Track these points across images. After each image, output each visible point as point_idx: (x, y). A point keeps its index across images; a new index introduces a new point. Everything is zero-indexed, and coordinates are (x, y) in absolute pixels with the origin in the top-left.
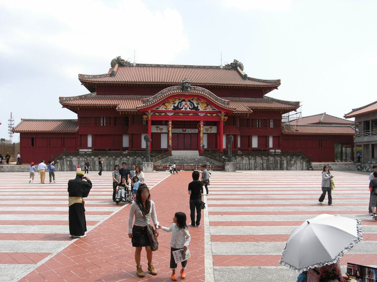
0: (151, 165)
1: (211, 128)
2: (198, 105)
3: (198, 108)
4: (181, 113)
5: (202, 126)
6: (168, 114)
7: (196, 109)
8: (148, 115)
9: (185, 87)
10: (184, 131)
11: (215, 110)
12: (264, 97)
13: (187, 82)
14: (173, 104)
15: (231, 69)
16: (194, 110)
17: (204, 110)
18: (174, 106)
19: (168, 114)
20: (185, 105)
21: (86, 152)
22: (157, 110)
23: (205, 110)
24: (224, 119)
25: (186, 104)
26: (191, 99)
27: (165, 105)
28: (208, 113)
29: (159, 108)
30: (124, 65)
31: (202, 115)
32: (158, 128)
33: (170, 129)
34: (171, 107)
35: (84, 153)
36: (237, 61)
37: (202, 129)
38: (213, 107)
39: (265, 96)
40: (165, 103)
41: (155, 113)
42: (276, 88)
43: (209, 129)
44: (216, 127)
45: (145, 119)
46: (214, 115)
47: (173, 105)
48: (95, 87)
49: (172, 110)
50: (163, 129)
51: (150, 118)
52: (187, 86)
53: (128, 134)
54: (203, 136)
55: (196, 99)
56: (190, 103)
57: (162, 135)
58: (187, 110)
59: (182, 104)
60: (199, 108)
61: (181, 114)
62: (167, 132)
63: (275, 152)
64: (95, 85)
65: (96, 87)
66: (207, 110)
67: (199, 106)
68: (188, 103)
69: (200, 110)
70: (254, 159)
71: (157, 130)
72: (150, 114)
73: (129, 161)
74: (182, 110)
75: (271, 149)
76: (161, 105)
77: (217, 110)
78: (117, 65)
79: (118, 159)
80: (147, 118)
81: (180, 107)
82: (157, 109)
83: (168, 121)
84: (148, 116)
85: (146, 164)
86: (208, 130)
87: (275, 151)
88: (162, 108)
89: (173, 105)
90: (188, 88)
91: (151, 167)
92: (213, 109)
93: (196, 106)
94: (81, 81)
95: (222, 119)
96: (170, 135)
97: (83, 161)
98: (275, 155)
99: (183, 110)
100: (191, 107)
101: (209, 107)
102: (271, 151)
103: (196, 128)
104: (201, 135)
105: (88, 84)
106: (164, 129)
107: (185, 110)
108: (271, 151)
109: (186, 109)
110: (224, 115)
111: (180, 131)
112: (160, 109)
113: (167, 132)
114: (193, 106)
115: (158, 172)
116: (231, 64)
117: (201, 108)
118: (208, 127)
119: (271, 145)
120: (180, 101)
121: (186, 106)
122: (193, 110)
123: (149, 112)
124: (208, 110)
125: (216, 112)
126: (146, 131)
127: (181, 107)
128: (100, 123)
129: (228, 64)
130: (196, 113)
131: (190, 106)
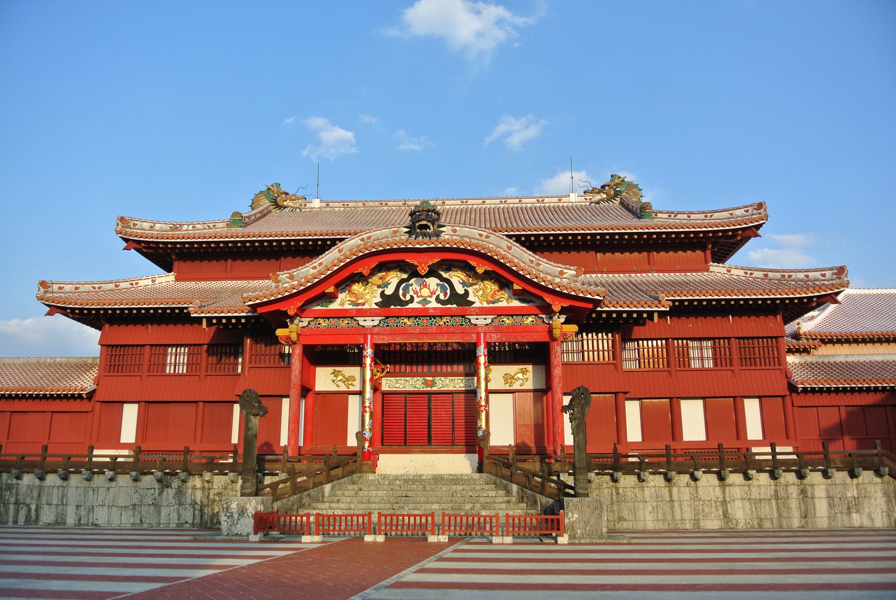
4: (409, 317)
5: (482, 360)
7: (462, 300)
10: (426, 383)
14: (379, 287)
15: (603, 200)
16: (455, 306)
17: (488, 303)
19: (361, 323)
23: (493, 303)
30: (285, 207)
31: (481, 321)
35: (108, 460)
36: (619, 177)
42: (750, 232)
44: (544, 367)
47: (381, 290)
56: (439, 282)
58: (427, 306)
59: (412, 285)
60: (471, 298)
61: (406, 320)
63: (774, 453)
67: (470, 290)
70: (688, 485)
71: (333, 381)
73: (212, 492)
74: (410, 306)
75: (757, 443)
79: (176, 483)
81: (404, 295)
83: (361, 349)
86: (512, 377)
87: (773, 449)
88: (342, 302)
89: (381, 290)
90: (427, 227)
93: (460, 290)
94: (126, 240)
97: (56, 489)
98: (774, 469)
99: (414, 305)
100: (442, 297)
102: (755, 450)
107: (420, 306)
108: (755, 450)
109: (425, 301)
112: (335, 306)
114: (448, 291)
116: (603, 187)
119: (754, 429)
120: (405, 276)
121: (425, 292)
122: (449, 306)
124: (504, 304)
127: (408, 298)
129: (594, 189)
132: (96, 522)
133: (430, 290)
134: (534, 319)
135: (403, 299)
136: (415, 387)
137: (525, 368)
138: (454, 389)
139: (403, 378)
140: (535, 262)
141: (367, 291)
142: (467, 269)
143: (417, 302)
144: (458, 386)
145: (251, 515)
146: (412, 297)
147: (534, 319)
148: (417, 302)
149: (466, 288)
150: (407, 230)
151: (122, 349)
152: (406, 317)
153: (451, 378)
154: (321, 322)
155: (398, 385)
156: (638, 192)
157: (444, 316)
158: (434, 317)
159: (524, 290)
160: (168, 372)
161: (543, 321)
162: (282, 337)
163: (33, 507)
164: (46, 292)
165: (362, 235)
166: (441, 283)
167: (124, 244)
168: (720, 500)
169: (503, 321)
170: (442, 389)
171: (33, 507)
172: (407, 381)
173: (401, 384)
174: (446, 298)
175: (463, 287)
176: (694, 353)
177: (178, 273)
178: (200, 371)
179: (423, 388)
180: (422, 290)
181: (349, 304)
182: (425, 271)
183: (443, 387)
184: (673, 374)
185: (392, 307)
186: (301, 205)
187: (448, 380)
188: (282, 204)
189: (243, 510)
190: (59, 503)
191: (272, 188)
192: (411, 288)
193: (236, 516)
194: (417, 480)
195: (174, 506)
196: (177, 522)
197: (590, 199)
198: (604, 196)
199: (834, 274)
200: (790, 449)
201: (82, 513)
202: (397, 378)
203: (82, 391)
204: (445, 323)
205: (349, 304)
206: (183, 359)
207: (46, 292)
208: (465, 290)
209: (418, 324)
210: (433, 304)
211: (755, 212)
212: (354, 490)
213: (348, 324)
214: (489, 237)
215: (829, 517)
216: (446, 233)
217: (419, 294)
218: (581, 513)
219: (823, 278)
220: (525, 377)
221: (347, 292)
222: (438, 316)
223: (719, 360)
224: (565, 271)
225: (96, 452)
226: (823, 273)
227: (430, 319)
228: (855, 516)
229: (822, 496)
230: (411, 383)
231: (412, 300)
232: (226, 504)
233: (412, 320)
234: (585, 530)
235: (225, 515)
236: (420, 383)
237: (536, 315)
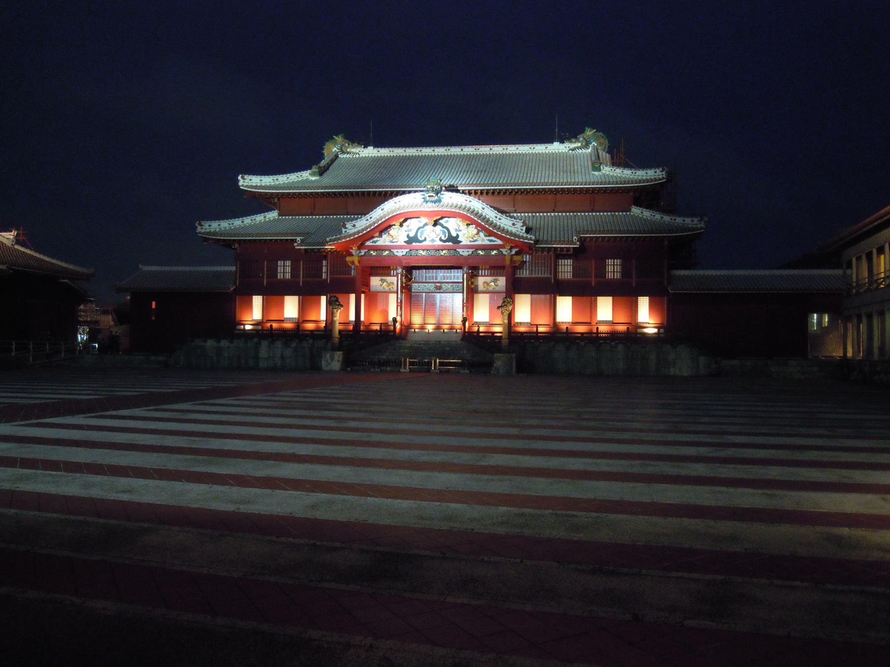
0: (339, 357)
3: (458, 239)
6: (395, 251)
11: (495, 243)
14: (406, 231)
15: (578, 148)
16: (451, 243)
18: (408, 236)
19: (395, 254)
23: (474, 241)
29: (377, 241)
32: (383, 283)
41: (369, 250)
43: (491, 282)
47: (407, 233)
61: (421, 252)
67: (460, 233)
69: (461, 244)
74: (424, 243)
77: (499, 242)
80: (353, 263)
81: (421, 237)
91: (338, 361)
100: (443, 238)
107: (430, 243)
109: (433, 241)
114: (447, 235)
122: (447, 243)
127: (423, 239)
130: (455, 249)
143: (430, 241)
144: (455, 289)
148: (430, 241)
149: (457, 232)
154: (372, 252)
155: (419, 289)
162: (349, 262)
164: (202, 229)
171: (214, 358)
175: (456, 231)
177: (279, 210)
193: (329, 361)
197: (569, 147)
208: (457, 234)
211: (660, 173)
219: (692, 223)
221: (387, 234)
231: (425, 240)
233: (425, 252)
237: (498, 250)
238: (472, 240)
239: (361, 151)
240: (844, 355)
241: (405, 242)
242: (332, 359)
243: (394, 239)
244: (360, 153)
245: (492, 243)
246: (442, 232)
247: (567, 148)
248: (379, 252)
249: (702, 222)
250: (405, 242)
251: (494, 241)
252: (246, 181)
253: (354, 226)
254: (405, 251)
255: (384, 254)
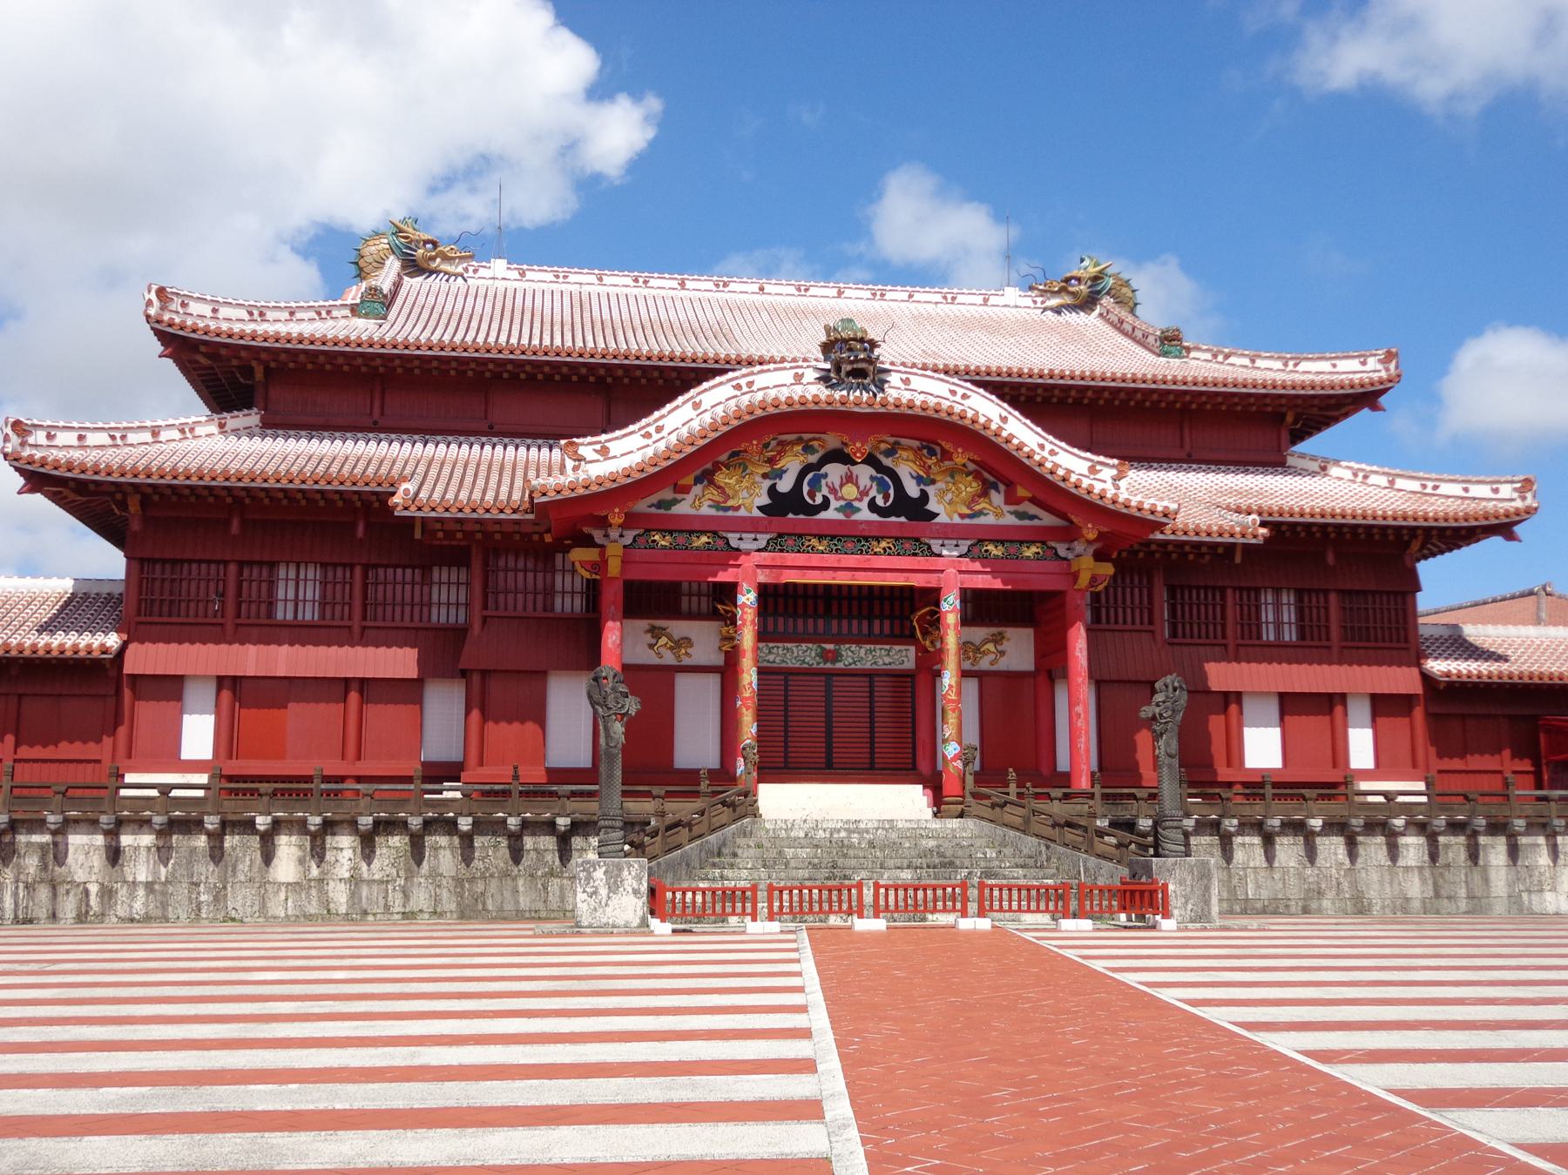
0: (640, 880)
1: (997, 639)
2: (926, 488)
4: (820, 537)
5: (952, 619)
7: (916, 509)
8: (603, 547)
9: (846, 368)
10: (825, 656)
11: (1036, 522)
12: (1291, 461)
13: (862, 340)
14: (765, 476)
16: (903, 519)
17: (962, 516)
18: (772, 491)
19: (734, 543)
20: (842, 485)
21: (165, 789)
22: (662, 511)
23: (971, 516)
24: (1094, 579)
25: (850, 479)
26: (883, 446)
27: (712, 483)
28: (991, 541)
29: (675, 502)
33: (747, 638)
34: (751, 497)
37: (951, 641)
38: (1019, 501)
39: (1302, 456)
40: (717, 467)
41: (647, 531)
43: (986, 641)
45: (587, 575)
46: (1030, 552)
47: (768, 483)
48: (248, 371)
49: (761, 515)
50: (692, 646)
51: (614, 567)
52: (863, 360)
53: (464, 674)
54: (959, 684)
55: (911, 448)
56: (874, 473)
57: (683, 683)
58: (857, 517)
59: (825, 476)
60: (932, 506)
62: (719, 660)
64: (254, 363)
65: (259, 375)
66: (982, 520)
67: (930, 490)
68: (864, 473)
69: (937, 520)
71: (651, 646)
72: (617, 542)
74: (823, 515)
76: (689, 480)
77: (1048, 519)
78: (393, 265)
80: (600, 566)
81: (812, 495)
82: (660, 505)
84: (602, 554)
85: (599, 874)
86: (977, 649)
88: (695, 504)
89: (768, 483)
91: (636, 892)
92: (1021, 515)
93: (913, 490)
94: (161, 335)
95: (1084, 580)
96: (749, 677)
99: (830, 514)
100: (880, 502)
101: (997, 498)
102: (1364, 786)
103: (906, 637)
104: (948, 679)
105: (205, 355)
106: (703, 641)
107: (840, 516)
108: (1364, 786)
109: (849, 508)
110: (1091, 550)
111: (801, 655)
112: (684, 508)
113: (719, 660)
114: (892, 492)
115: (689, 931)
117: (944, 506)
118: (978, 634)
120: (813, 459)
121: (850, 491)
122: (893, 519)
123: (616, 519)
124: (989, 519)
125: (1041, 536)
126: (588, 655)
127: (819, 500)
128: (271, 604)
130: (916, 535)
131: (873, 493)
132: (233, 914)
133: (858, 488)
134: (1039, 550)
135: (810, 502)
136: (803, 661)
137: (1000, 633)
138: (874, 667)
139: (780, 645)
140: (1048, 447)
141: (744, 484)
142: (925, 451)
143: (836, 509)
144: (881, 662)
145: (630, 891)
146: (826, 499)
147: (1039, 550)
148: (836, 509)
149: (922, 487)
150: (823, 373)
151: (168, 566)
152: (815, 536)
153: (868, 647)
154: (657, 537)
155: (771, 658)
156: (1130, 294)
157: (883, 538)
158: (866, 539)
159: (1033, 497)
160: (280, 616)
161: (1056, 553)
163: (94, 889)
164: (23, 444)
165: (737, 378)
166: (879, 475)
167: (158, 347)
168: (1345, 867)
169: (987, 551)
170: (853, 666)
171: (94, 889)
172: (788, 649)
173: (778, 655)
174: (888, 504)
175: (919, 485)
176: (1268, 615)
178: (349, 619)
179: (818, 664)
180: (844, 489)
181: (710, 506)
182: (863, 454)
183: (854, 663)
184: (1231, 648)
185: (791, 516)
186: (466, 270)
187: (863, 651)
188: (426, 266)
189: (616, 881)
190: (150, 879)
191: (402, 226)
192: (823, 482)
194: (853, 827)
195: (395, 881)
196: (403, 910)
198: (1068, 300)
199: (1515, 490)
200: (1421, 786)
201: (203, 898)
202: (771, 645)
203: (103, 653)
204: (884, 549)
205: (710, 506)
206: (311, 592)
207: (23, 444)
209: (836, 550)
210: (865, 514)
211: (1379, 367)
212: (749, 846)
213: (709, 543)
214: (969, 397)
215: (1510, 896)
216: (892, 385)
217: (839, 494)
218: (1182, 882)
219: (1494, 496)
220: (1000, 648)
221: (706, 482)
222: (873, 537)
223: (1307, 630)
224: (1098, 467)
225: (130, 778)
226: (1495, 486)
227: (859, 541)
228: (1549, 896)
229: (1501, 863)
230: (795, 654)
231: (826, 504)
232: (584, 870)
234: (1186, 910)
235: (584, 891)
236: (813, 654)
237: (1044, 543)
238: (968, 512)
239: (471, 269)
240: (1314, 842)
241: (759, 508)
242: (614, 885)
243: (728, 498)
244: (465, 275)
245: (1027, 522)
246: (874, 484)
247: (1039, 305)
248: (681, 539)
249: (1529, 495)
250: (759, 508)
251: (1033, 517)
252: (173, 307)
253: (604, 451)
254: (763, 539)
255: (695, 544)
